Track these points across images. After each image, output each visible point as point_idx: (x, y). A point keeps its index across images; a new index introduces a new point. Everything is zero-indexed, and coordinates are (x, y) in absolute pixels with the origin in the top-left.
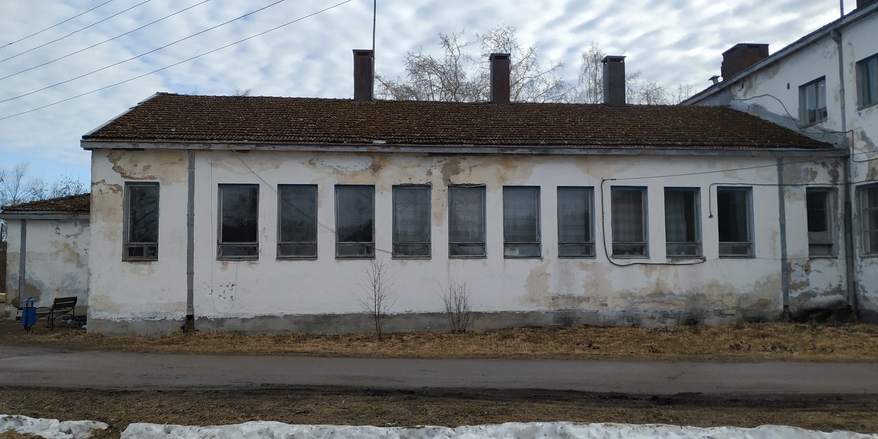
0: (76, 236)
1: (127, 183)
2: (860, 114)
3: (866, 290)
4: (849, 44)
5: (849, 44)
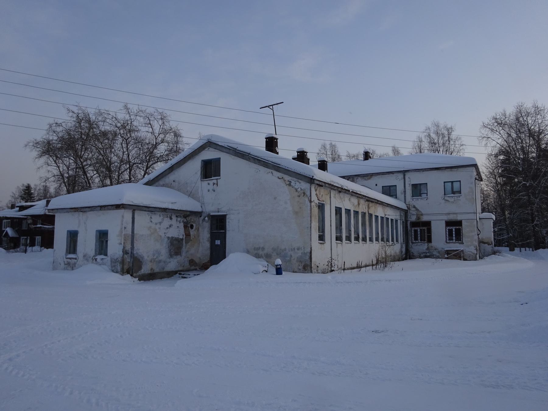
0: (160, 223)
1: (319, 203)
2: (413, 200)
3: (414, 253)
4: (409, 178)
5: (409, 178)
